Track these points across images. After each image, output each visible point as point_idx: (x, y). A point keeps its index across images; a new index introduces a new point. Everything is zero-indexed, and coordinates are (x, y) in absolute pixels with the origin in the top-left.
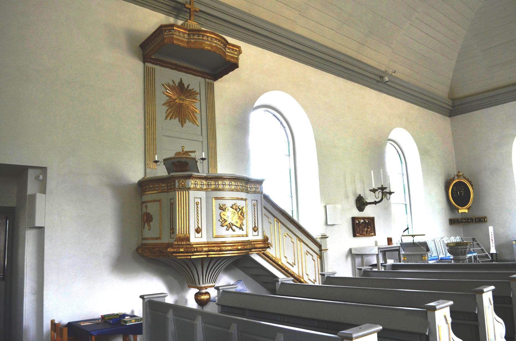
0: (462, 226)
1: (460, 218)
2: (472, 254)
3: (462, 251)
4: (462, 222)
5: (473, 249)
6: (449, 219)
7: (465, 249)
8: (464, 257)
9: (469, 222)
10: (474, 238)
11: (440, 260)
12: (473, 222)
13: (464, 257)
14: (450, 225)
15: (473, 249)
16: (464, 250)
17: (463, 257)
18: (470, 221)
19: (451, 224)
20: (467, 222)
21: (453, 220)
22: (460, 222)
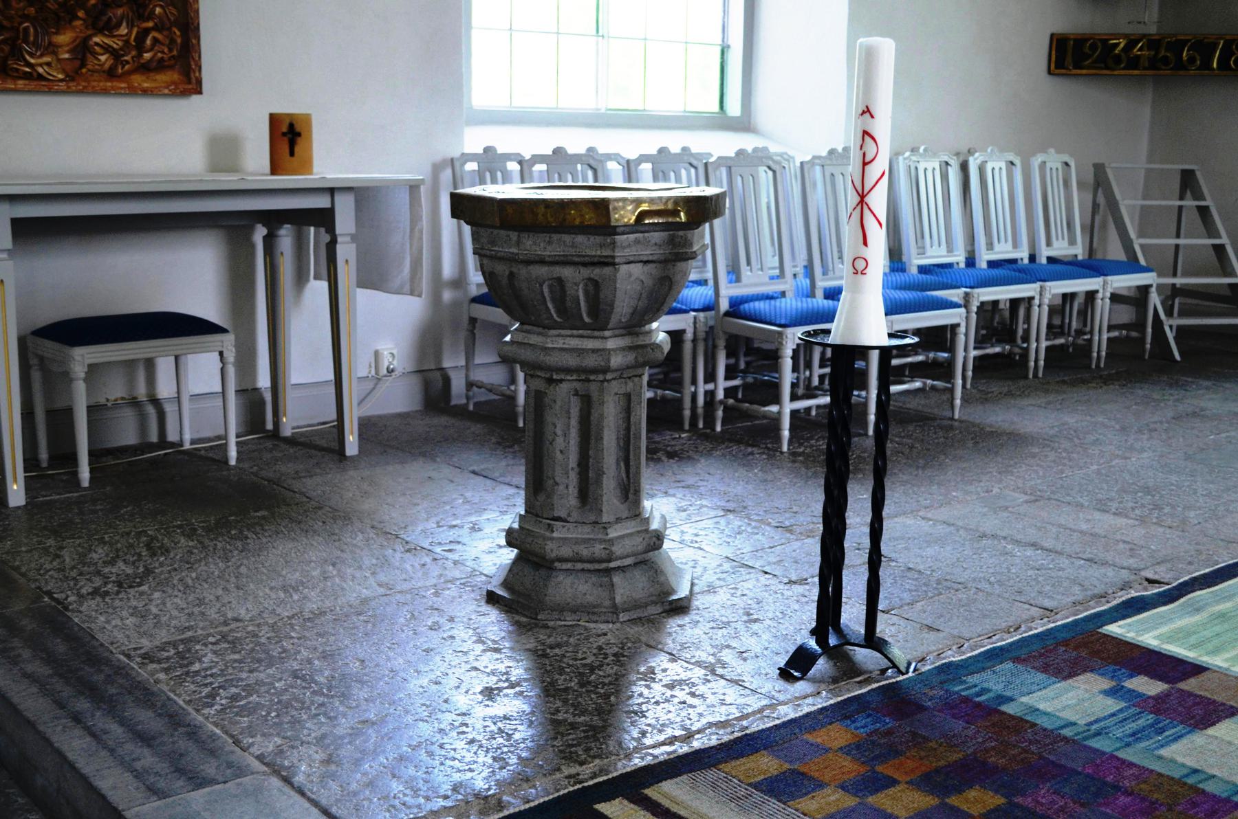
0: (1149, 95)
1: (1125, 36)
2: (1100, 280)
3: (560, 281)
4: (1134, 63)
5: (1181, 241)
6: (1052, 35)
7: (596, 272)
8: (590, 344)
9: (1180, 66)
10: (1192, 172)
11: (727, 314)
12: (1206, 65)
13: (590, 344)
14: (1049, 72)
15: (1181, 241)
16: (586, 272)
17: (580, 352)
18: (1192, 60)
19: (1057, 67)
20: (1165, 61)
21: (1076, 40)
22: (1118, 60)
